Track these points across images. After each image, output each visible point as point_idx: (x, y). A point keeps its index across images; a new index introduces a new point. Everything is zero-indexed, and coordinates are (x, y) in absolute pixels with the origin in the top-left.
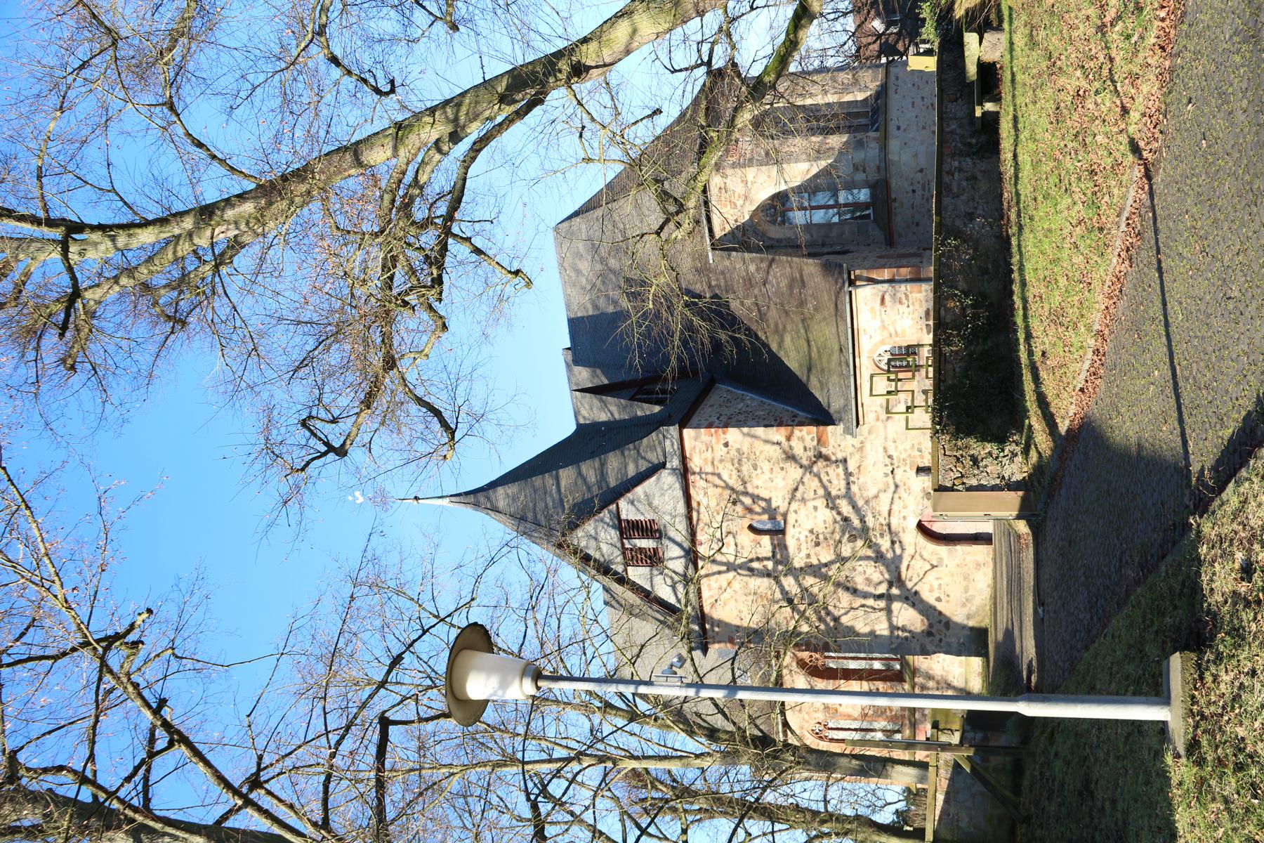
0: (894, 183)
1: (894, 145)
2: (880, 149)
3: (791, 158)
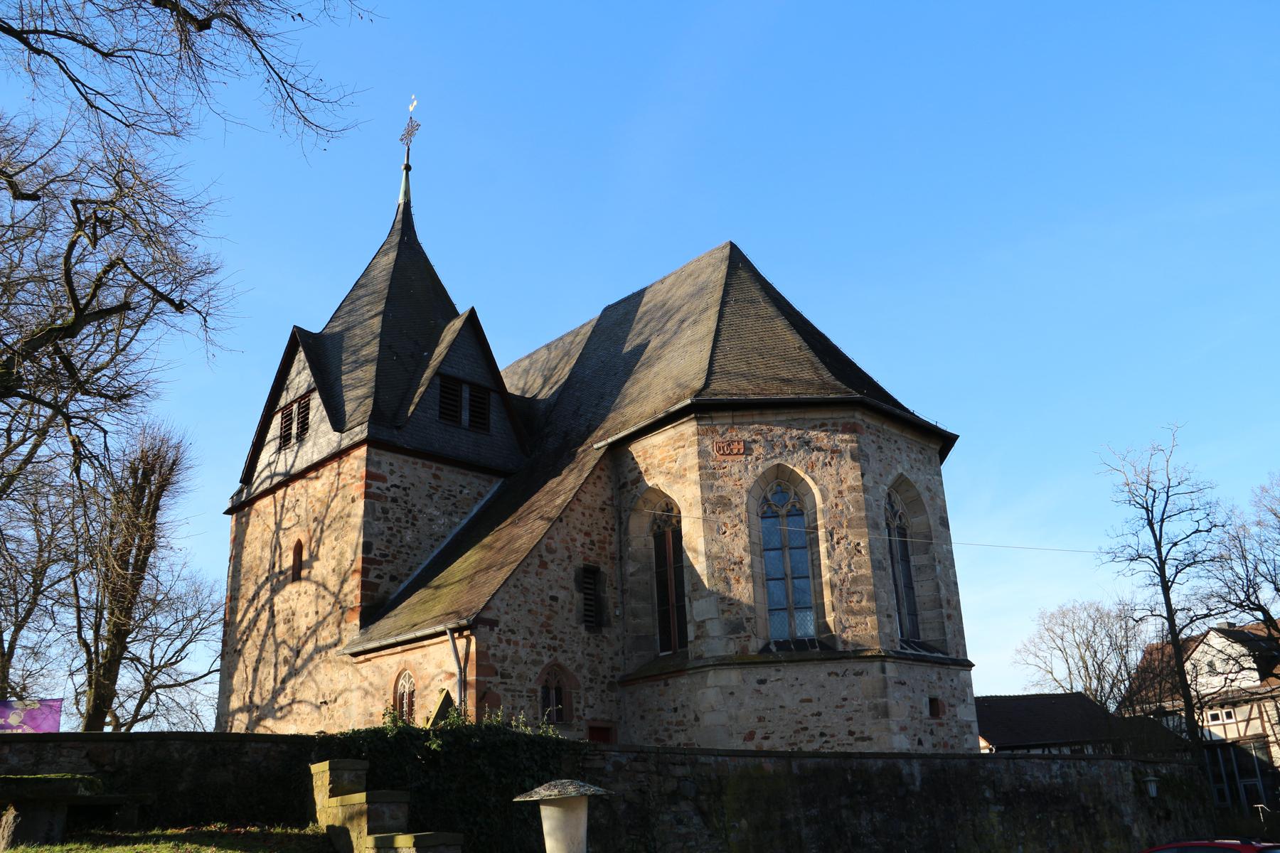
0: (684, 680)
1: (732, 677)
2: (724, 658)
3: (712, 529)
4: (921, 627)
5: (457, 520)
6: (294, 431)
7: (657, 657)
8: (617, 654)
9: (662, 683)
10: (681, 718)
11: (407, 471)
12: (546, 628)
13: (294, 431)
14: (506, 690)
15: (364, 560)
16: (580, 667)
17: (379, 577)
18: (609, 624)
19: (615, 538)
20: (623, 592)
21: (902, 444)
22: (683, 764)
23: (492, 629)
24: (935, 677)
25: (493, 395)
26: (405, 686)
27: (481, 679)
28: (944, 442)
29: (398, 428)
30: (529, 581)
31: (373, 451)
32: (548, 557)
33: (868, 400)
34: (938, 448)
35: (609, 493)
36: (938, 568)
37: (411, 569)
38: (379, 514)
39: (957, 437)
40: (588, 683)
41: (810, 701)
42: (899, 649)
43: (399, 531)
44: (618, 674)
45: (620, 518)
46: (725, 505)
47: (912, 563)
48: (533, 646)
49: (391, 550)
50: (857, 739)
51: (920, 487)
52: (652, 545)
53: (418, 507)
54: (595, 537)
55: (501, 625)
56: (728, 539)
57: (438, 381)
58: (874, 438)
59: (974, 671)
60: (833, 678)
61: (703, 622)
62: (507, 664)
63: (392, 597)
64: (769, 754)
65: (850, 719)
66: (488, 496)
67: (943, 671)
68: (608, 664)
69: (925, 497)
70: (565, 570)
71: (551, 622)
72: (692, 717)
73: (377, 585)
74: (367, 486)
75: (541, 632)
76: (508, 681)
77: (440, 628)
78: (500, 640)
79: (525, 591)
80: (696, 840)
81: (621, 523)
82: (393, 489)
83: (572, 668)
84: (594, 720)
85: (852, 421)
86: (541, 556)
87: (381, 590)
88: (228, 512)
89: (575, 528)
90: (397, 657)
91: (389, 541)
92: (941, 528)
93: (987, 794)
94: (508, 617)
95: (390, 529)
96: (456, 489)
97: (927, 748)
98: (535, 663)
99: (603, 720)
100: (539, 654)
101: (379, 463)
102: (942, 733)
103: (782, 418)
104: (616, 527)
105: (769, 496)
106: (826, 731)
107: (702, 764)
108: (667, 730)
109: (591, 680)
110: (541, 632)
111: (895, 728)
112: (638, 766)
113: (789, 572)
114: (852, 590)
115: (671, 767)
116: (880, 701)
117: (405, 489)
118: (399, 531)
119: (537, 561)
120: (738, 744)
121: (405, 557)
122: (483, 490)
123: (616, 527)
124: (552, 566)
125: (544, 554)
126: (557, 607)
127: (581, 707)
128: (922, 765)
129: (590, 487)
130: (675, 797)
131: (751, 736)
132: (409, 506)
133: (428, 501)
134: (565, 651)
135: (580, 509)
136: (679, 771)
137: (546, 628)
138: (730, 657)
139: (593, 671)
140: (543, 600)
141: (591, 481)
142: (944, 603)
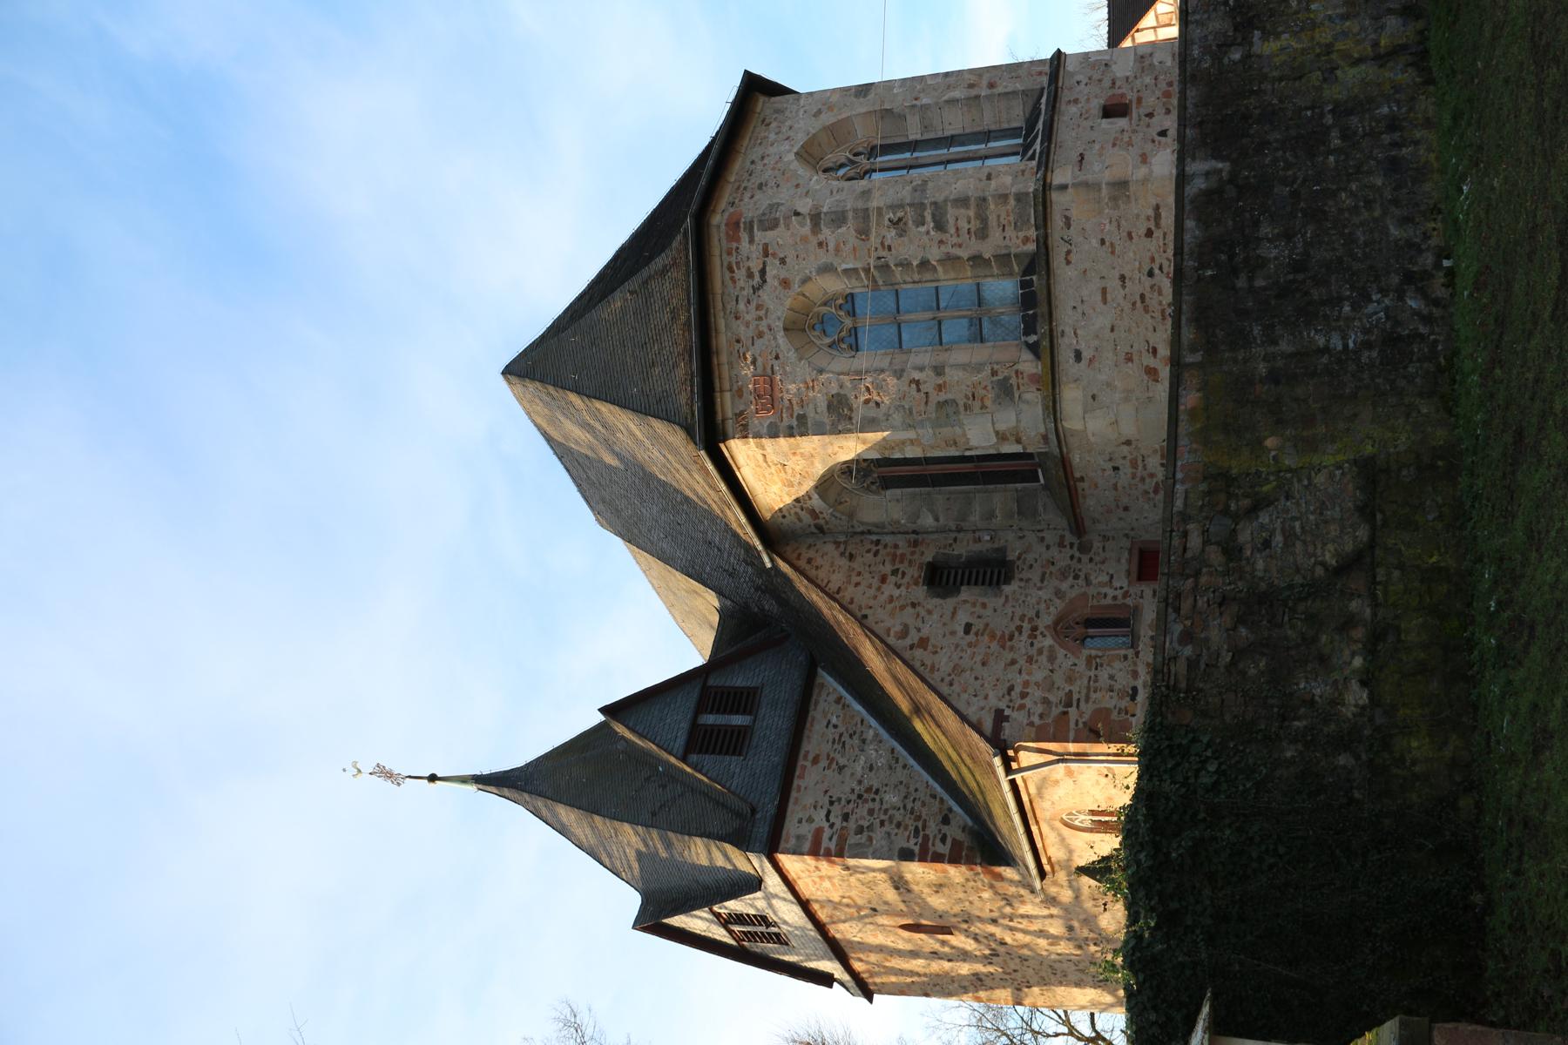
0: (1076, 459)
1: (1071, 397)
2: (1045, 408)
4: (1005, 126)
5: (871, 732)
6: (763, 929)
7: (1046, 487)
8: (1042, 539)
9: (1080, 485)
10: (1127, 463)
11: (809, 800)
12: (1006, 640)
13: (763, 929)
14: (1087, 699)
15: (922, 859)
16: (1058, 593)
17: (943, 840)
18: (1002, 551)
19: (888, 539)
20: (959, 530)
21: (756, 153)
22: (1185, 534)
23: (1007, 719)
24: (1073, 109)
25: (711, 682)
26: (1085, 820)
27: (1072, 735)
28: (754, 89)
29: (754, 811)
30: (944, 662)
31: (782, 845)
32: (913, 637)
33: (694, 207)
34: (762, 99)
35: (830, 548)
36: (925, 101)
37: (934, 796)
38: (863, 838)
39: (746, 72)
40: (1081, 582)
41: (1104, 291)
42: (1034, 163)
43: (886, 811)
44: (1069, 538)
45: (862, 533)
46: (840, 402)
47: (919, 137)
48: (1030, 660)
49: (910, 822)
50: (1158, 225)
51: (814, 126)
52: (898, 491)
53: (854, 785)
54: (888, 568)
55: (1002, 705)
56: (886, 400)
57: (694, 758)
58: (747, 195)
59: (1068, 49)
60: (1073, 257)
61: (997, 433)
62: (1052, 698)
63: (970, 823)
64: (1174, 400)
65: (1130, 235)
66: (840, 689)
67: (1065, 96)
68: (1054, 552)
69: (828, 119)
70: (930, 612)
71: (999, 634)
72: (1125, 449)
73: (955, 843)
74: (828, 855)
75: (1012, 648)
76: (1075, 697)
77: (1006, 787)
78: (1022, 707)
79: (957, 670)
80: (1294, 519)
81: (869, 532)
82: (832, 819)
83: (1059, 605)
84: (1129, 573)
85: (723, 227)
86: (912, 647)
87: (960, 836)
88: (871, 1001)
89: (875, 597)
90: (1045, 828)
91: (899, 825)
92: (871, 96)
93: (1237, 56)
94: (991, 694)
95: (882, 823)
96: (831, 733)
97: (1171, 123)
98: (1052, 659)
99: (1129, 561)
100: (1040, 652)
101: (799, 837)
102: (1150, 101)
103: (722, 323)
104: (874, 538)
105: (828, 341)
106: (1146, 269)
107: (1185, 504)
108: (1143, 479)
109: (1076, 577)
110: (1012, 648)
111: (1142, 171)
112: (1186, 606)
113: (929, 315)
114: (952, 231)
115: (1189, 554)
116: (1105, 191)
117: (832, 803)
118: (886, 811)
119: (918, 653)
120: (1162, 390)
121: (918, 804)
122: (832, 698)
123: (874, 538)
124: (925, 632)
125: (908, 641)
126: (978, 625)
127: (1111, 593)
128: (1194, 159)
129: (822, 575)
130: (1231, 551)
131: (1152, 372)
132: (854, 797)
133: (847, 772)
134: (1038, 616)
135: (851, 588)
136: (1195, 541)
137: (1006, 640)
138: (1044, 398)
139: (1063, 575)
140: (970, 645)
141: (812, 573)
142: (973, 92)
